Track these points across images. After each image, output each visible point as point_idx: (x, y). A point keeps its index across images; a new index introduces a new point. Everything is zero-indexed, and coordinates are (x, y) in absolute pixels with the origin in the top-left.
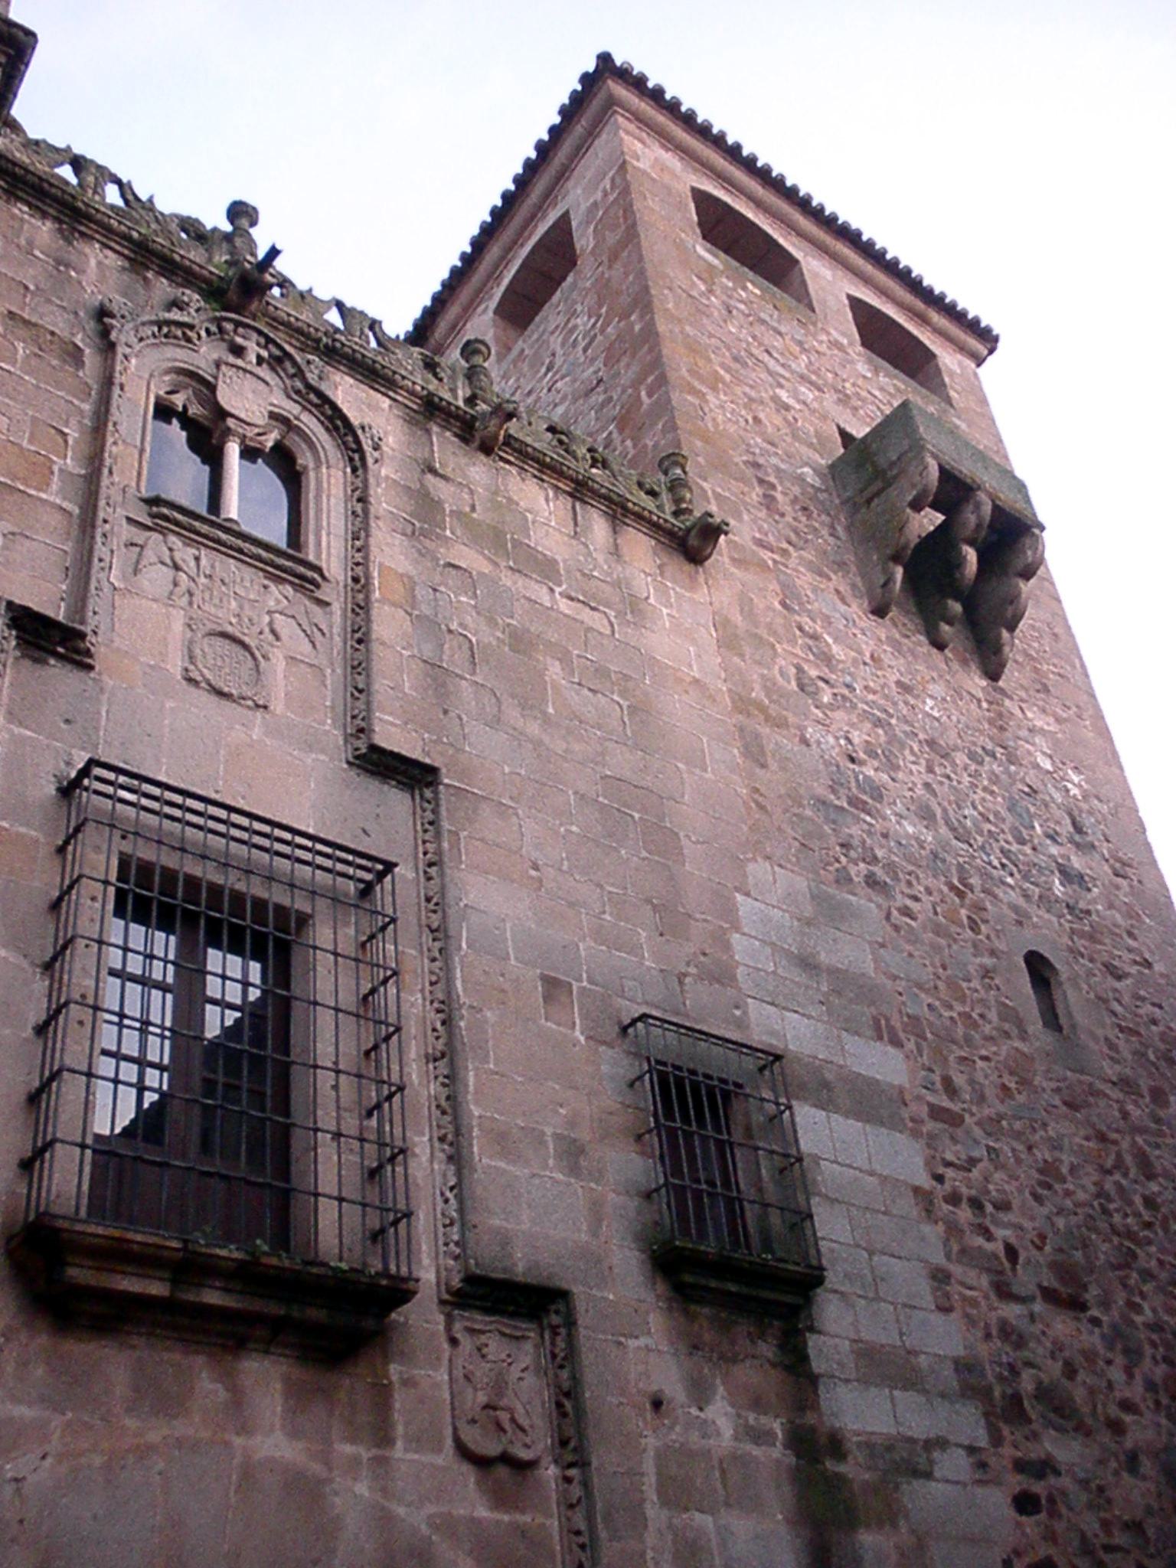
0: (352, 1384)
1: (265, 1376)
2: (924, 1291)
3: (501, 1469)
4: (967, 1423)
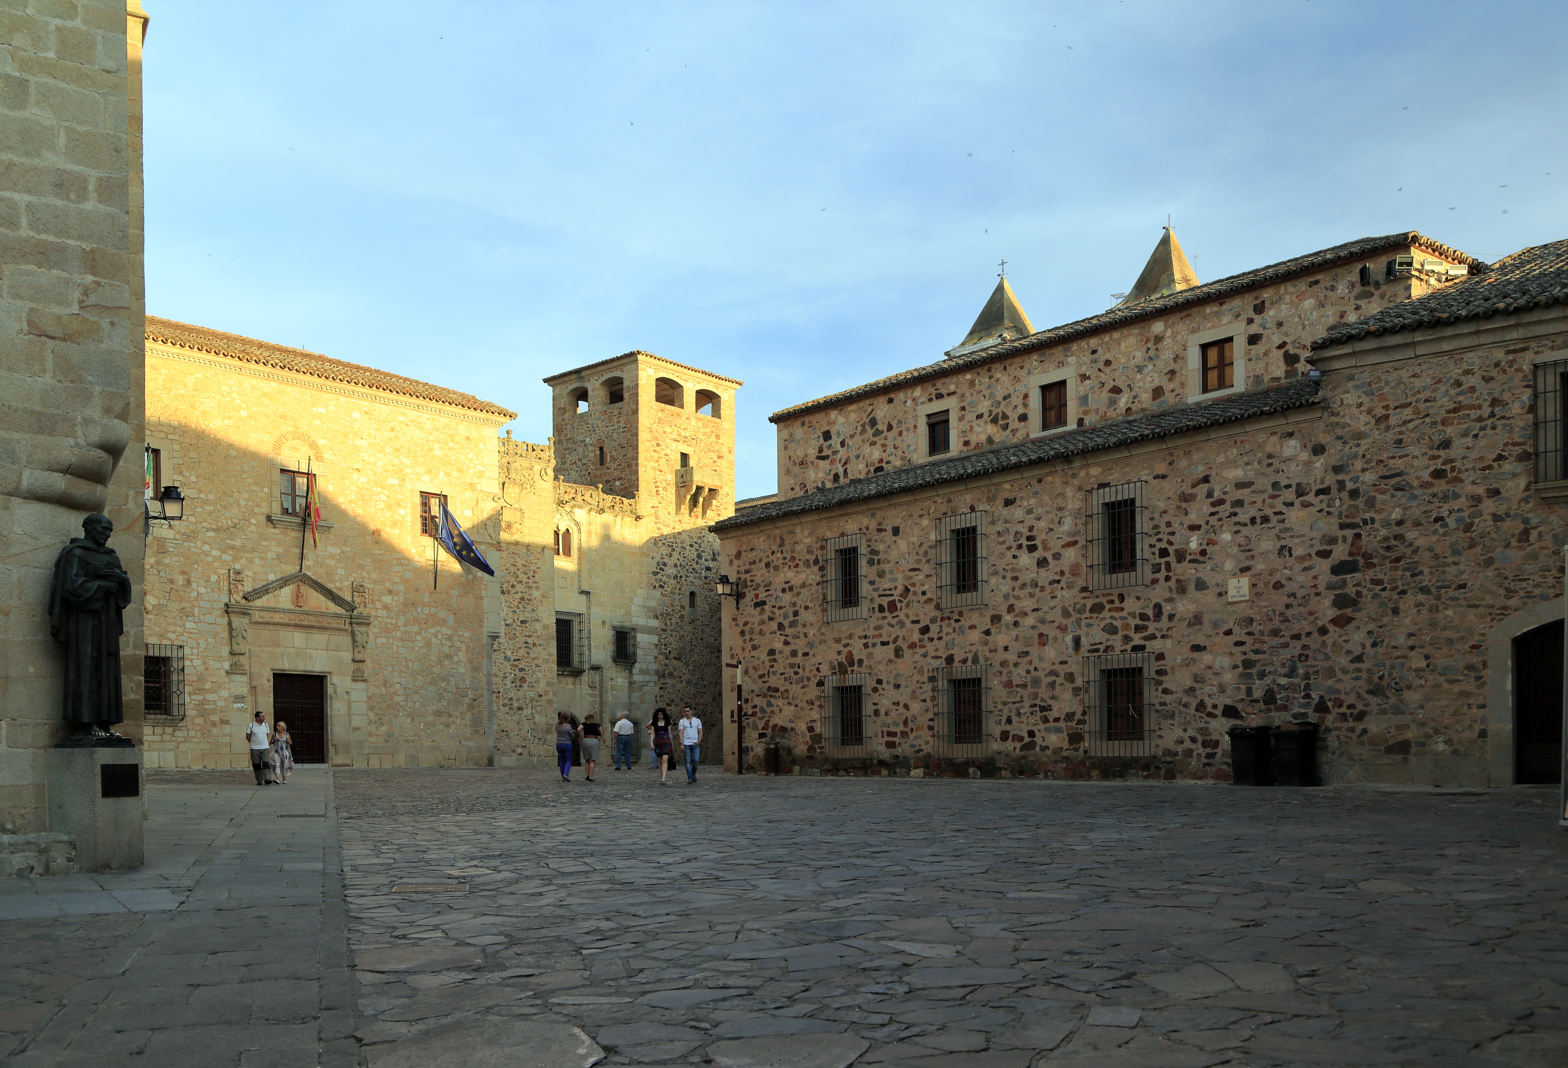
0: (578, 679)
1: (570, 680)
2: (652, 660)
3: (592, 687)
4: (655, 678)
